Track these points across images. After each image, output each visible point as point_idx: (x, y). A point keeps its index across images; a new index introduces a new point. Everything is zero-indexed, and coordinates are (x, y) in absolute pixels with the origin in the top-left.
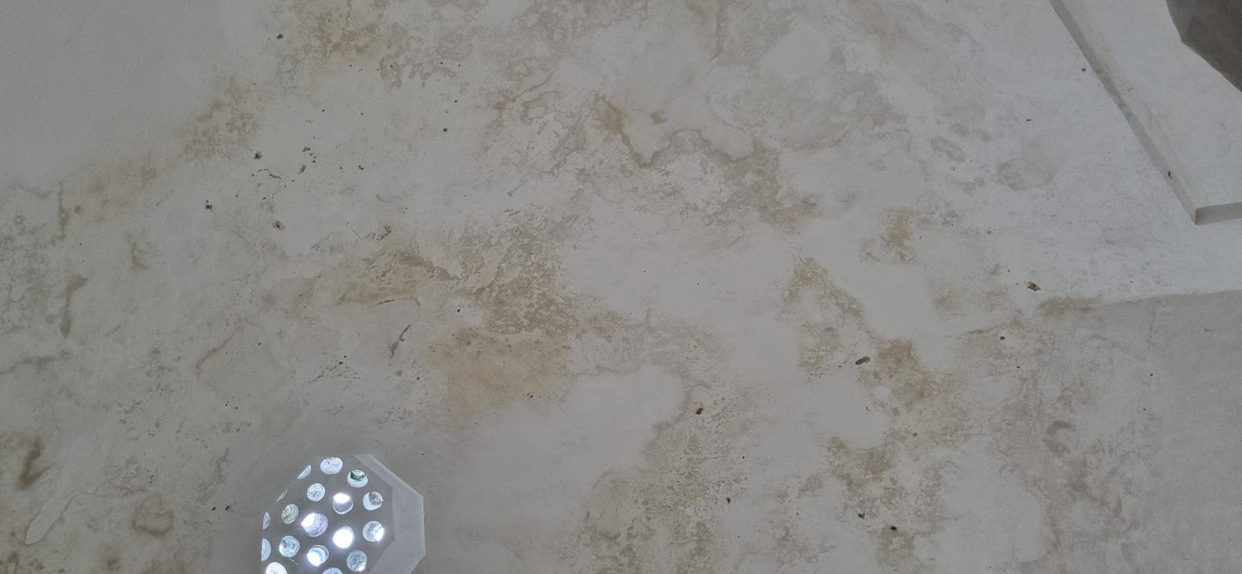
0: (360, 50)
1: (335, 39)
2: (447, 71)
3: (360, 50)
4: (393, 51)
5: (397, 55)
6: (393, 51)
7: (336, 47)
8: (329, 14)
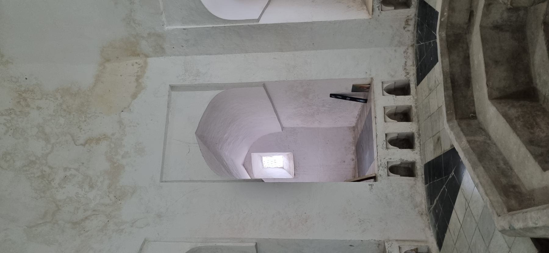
0: (19, 102)
1: (24, 95)
2: (7, 132)
3: (19, 102)
4: (18, 113)
5: (15, 114)
6: (18, 113)
7: (20, 95)
8: (34, 93)
